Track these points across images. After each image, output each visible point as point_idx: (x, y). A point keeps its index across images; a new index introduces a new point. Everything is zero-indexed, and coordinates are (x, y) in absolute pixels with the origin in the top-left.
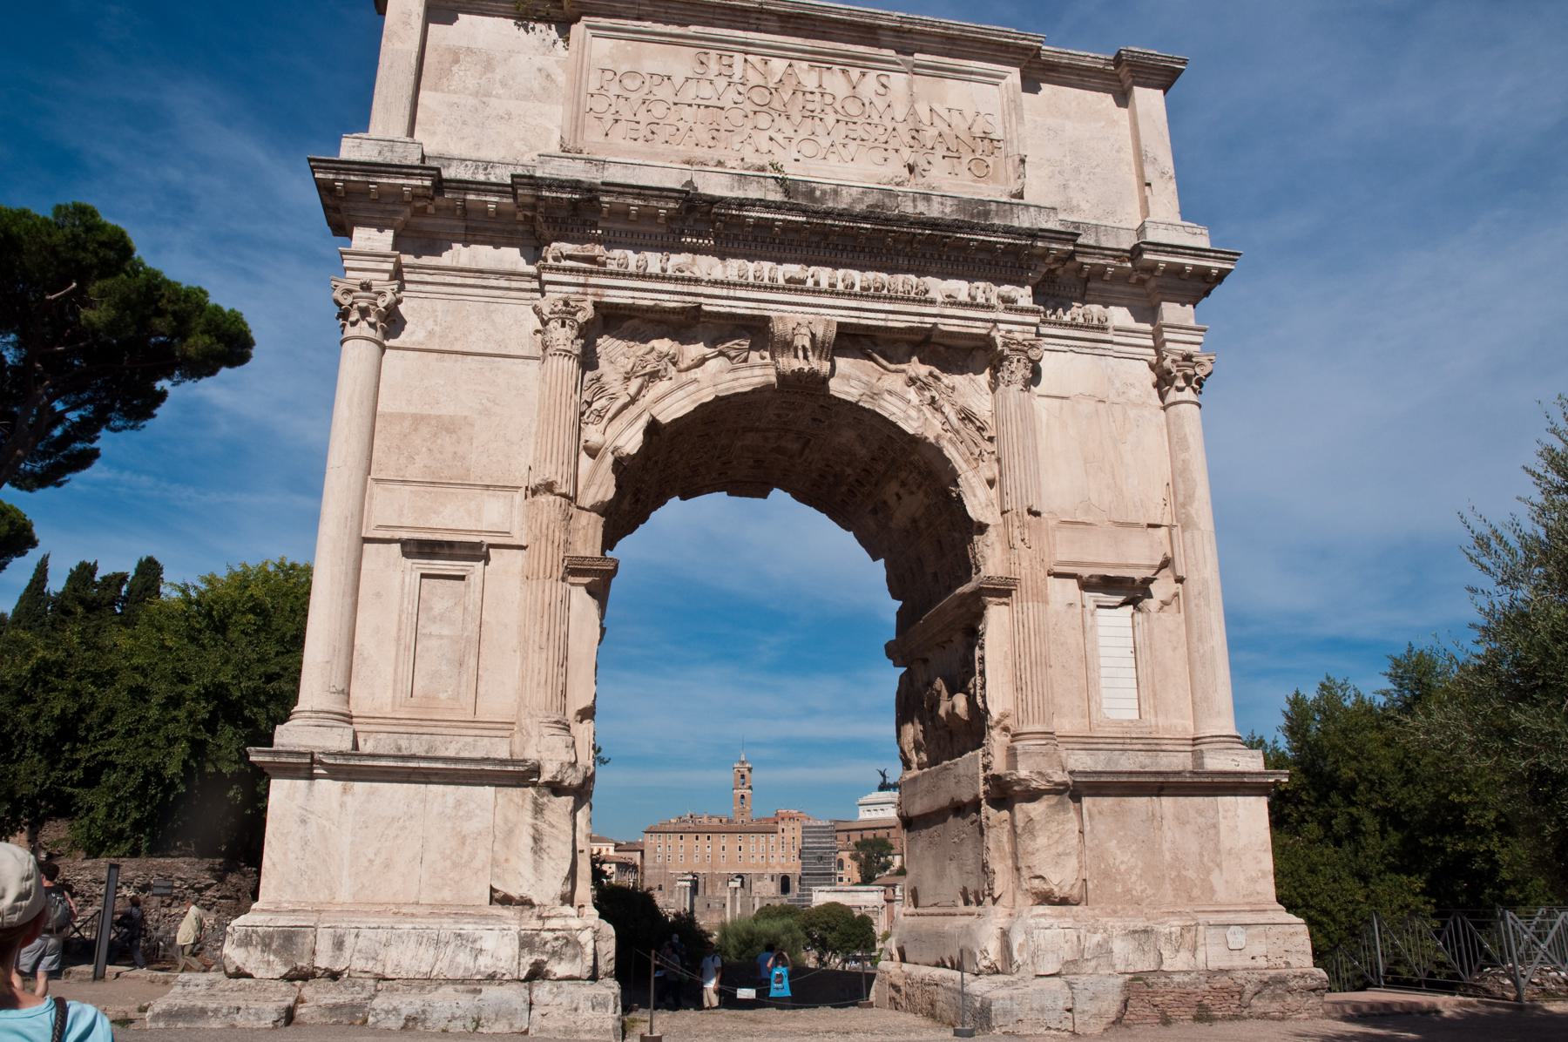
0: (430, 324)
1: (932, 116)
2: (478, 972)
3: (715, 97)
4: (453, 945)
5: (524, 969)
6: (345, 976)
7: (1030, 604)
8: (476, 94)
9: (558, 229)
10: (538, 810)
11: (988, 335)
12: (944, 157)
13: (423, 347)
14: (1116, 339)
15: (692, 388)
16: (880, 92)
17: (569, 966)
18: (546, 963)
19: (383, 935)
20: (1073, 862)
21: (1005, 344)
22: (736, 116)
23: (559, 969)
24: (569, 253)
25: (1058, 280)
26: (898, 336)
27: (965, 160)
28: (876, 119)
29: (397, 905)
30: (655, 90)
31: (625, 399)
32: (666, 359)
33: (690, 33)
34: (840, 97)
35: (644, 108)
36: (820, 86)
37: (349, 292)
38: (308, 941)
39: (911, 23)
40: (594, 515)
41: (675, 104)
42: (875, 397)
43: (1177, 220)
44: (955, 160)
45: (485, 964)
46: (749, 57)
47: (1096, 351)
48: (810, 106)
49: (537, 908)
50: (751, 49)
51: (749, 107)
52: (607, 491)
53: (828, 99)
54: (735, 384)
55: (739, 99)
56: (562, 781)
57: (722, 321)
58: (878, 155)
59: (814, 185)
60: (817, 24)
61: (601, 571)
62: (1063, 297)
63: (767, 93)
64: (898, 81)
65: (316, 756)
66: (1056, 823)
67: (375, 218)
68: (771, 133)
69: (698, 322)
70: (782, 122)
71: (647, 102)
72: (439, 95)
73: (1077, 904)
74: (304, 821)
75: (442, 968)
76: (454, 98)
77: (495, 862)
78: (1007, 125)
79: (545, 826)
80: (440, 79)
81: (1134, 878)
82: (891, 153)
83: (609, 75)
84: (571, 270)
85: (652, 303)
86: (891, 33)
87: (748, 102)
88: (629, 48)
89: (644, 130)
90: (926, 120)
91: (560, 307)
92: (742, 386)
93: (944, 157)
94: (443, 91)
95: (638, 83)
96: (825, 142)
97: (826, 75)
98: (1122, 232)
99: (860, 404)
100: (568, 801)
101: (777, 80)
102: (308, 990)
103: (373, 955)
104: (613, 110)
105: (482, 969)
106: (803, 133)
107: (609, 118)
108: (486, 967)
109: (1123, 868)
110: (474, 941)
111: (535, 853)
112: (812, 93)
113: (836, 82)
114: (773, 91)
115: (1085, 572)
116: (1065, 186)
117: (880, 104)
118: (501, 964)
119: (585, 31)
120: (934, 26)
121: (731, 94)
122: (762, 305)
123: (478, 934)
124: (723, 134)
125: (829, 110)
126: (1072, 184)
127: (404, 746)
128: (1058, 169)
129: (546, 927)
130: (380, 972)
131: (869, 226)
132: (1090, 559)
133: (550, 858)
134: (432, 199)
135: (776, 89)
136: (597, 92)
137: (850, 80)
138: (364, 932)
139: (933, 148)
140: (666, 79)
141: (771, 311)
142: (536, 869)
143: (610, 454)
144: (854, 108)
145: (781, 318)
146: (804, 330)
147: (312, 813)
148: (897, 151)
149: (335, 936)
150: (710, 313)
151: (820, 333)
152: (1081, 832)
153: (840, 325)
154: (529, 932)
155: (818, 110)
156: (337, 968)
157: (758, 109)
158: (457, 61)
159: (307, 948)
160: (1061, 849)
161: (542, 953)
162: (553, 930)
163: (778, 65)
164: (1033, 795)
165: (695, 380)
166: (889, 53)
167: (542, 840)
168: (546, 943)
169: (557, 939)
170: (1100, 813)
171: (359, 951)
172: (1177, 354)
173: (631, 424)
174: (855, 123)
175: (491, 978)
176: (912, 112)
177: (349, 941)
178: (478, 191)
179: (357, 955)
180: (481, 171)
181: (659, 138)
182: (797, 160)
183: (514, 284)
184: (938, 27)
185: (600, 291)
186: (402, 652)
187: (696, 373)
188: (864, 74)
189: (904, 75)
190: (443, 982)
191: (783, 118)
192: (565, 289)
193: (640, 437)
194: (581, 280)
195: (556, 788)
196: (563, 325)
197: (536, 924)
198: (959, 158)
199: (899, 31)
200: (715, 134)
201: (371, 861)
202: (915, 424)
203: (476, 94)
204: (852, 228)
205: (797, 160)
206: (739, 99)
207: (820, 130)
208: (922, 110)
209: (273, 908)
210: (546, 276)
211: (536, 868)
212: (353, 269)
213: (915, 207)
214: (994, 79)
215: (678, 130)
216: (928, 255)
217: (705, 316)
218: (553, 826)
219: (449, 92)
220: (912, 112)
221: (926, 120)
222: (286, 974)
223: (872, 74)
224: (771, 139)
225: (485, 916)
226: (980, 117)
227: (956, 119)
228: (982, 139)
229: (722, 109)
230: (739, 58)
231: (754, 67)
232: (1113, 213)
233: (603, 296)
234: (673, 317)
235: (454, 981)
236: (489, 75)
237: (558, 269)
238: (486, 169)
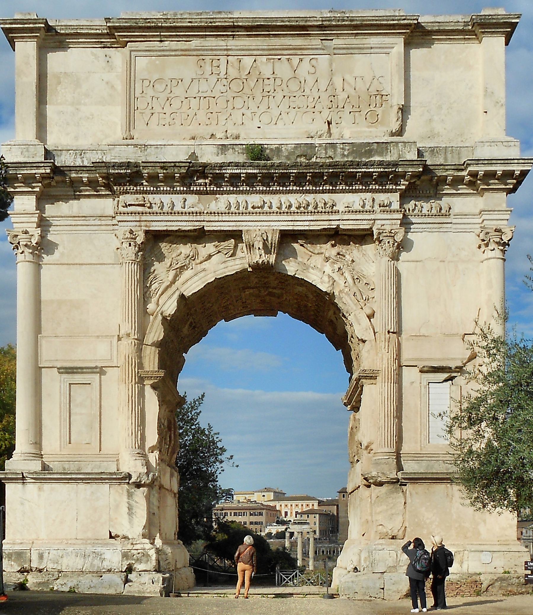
2: (104, 568)
3: (209, 91)
4: (91, 557)
5: (124, 567)
6: (45, 570)
7: (386, 384)
10: (130, 495)
11: (371, 228)
12: (350, 113)
14: (454, 221)
15: (202, 274)
17: (145, 565)
18: (134, 564)
19: (60, 553)
20: (400, 518)
21: (379, 234)
22: (221, 102)
23: (140, 567)
24: (130, 203)
25: (418, 187)
26: (319, 233)
27: (364, 113)
28: (307, 92)
29: (67, 540)
33: (192, 48)
36: (274, 73)
38: (27, 556)
39: (329, 21)
40: (153, 348)
41: (187, 98)
42: (305, 271)
43: (502, 136)
44: (357, 114)
45: (106, 565)
47: (441, 230)
49: (131, 540)
50: (230, 53)
51: (230, 94)
52: (159, 335)
53: (278, 82)
54: (226, 270)
56: (140, 481)
57: (218, 234)
58: (308, 118)
59: (266, 146)
61: (158, 377)
64: (323, 60)
65: (24, 475)
66: (391, 499)
68: (244, 110)
69: (206, 235)
70: (251, 103)
71: (170, 99)
73: (403, 539)
74: (22, 504)
75: (87, 567)
77: (111, 520)
78: (393, 84)
79: (133, 502)
81: (434, 526)
88: (157, 62)
89: (168, 119)
91: (127, 236)
92: (229, 271)
95: (164, 86)
96: (275, 112)
97: (277, 64)
99: (296, 276)
100: (144, 491)
102: (29, 577)
103: (57, 562)
105: (105, 567)
106: (263, 108)
107: (148, 112)
108: (107, 566)
109: (428, 521)
110: (101, 555)
111: (129, 515)
112: (268, 79)
114: (245, 81)
115: (421, 365)
117: (311, 80)
118: (114, 565)
120: (344, 20)
121: (220, 87)
123: (102, 552)
125: (278, 89)
127: (66, 468)
129: (134, 548)
130: (60, 569)
131: (296, 171)
132: (425, 356)
133: (136, 517)
134: (53, 178)
136: (140, 95)
137: (292, 67)
138: (51, 552)
139: (344, 107)
140: (180, 81)
142: (130, 522)
143: (160, 315)
145: (247, 231)
146: (259, 238)
147: (25, 500)
149: (39, 554)
150: (209, 231)
152: (405, 503)
153: (280, 230)
154: (126, 551)
156: (41, 567)
159: (28, 559)
160: (393, 511)
161: (132, 560)
162: (137, 550)
163: (248, 61)
164: (380, 484)
165: (204, 270)
166: (316, 42)
167: (132, 509)
168: (134, 555)
169: (139, 553)
170: (417, 493)
171: (50, 560)
173: (170, 298)
174: (295, 97)
175: (109, 571)
176: (331, 83)
177: (46, 555)
178: (77, 172)
179: (49, 561)
181: (178, 122)
182: (259, 127)
183: (103, 223)
185: (148, 224)
186: (62, 423)
187: (205, 265)
188: (301, 60)
190: (88, 573)
193: (175, 304)
195: (138, 485)
196: (130, 244)
197: (130, 547)
199: (322, 27)
201: (54, 521)
202: (327, 285)
204: (286, 173)
205: (259, 127)
206: (224, 89)
207: (273, 105)
208: (338, 82)
209: (11, 542)
210: (119, 218)
211: (131, 521)
213: (326, 153)
214: (386, 50)
216: (334, 183)
217: (208, 232)
218: (137, 503)
220: (331, 83)
222: (19, 570)
223: (307, 59)
225: (107, 544)
227: (360, 84)
228: (376, 96)
229: (214, 97)
230: (223, 59)
232: (461, 135)
233: (150, 226)
235: (93, 572)
238: (81, 155)
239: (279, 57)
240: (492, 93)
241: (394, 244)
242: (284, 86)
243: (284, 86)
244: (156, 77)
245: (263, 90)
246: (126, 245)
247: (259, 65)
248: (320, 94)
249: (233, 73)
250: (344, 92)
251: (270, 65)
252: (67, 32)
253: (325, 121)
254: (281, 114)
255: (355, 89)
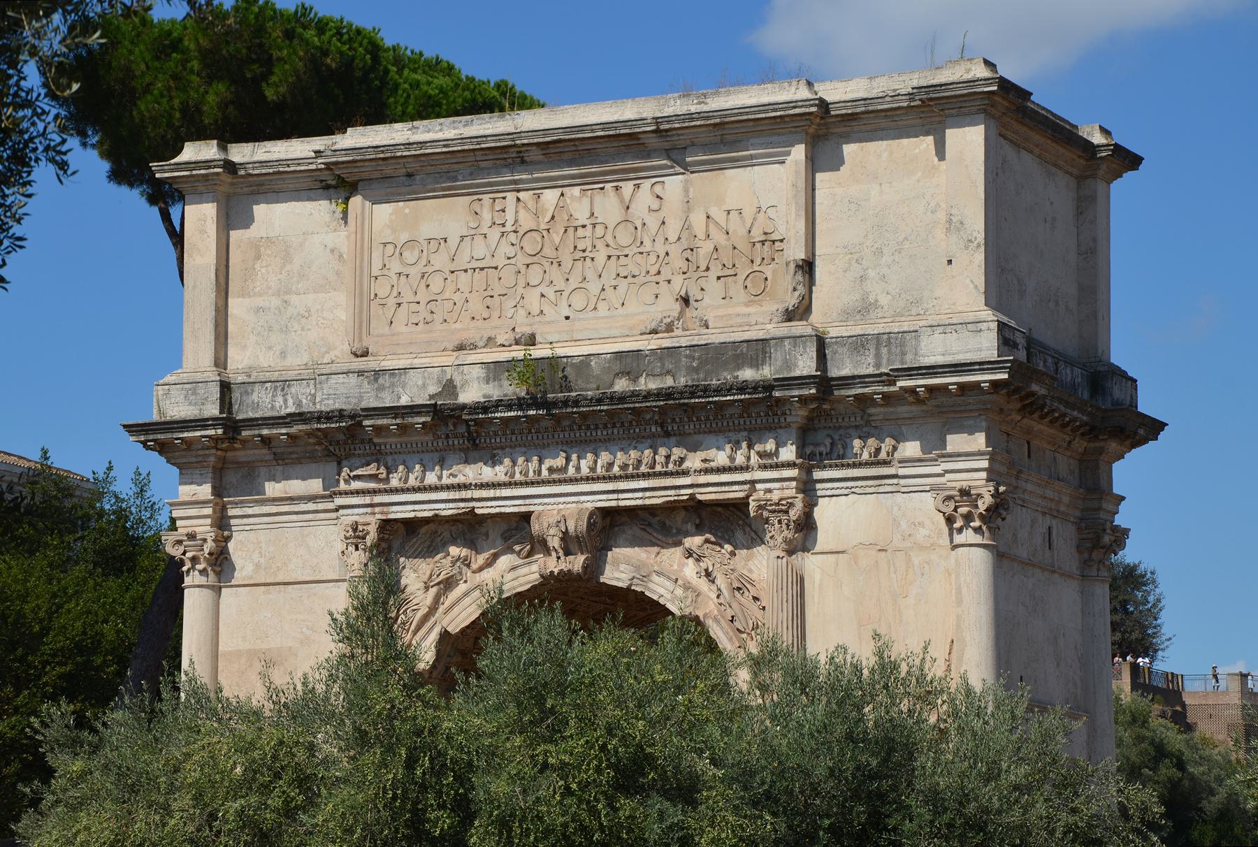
0: (256, 557)
1: (707, 226)
3: (489, 256)
8: (278, 294)
9: (342, 450)
13: (252, 582)
16: (652, 208)
22: (508, 275)
28: (648, 246)
30: (432, 257)
31: (424, 610)
32: (458, 564)
34: (611, 227)
35: (423, 282)
37: (179, 542)
39: (668, 122)
41: (452, 272)
44: (731, 278)
46: (522, 195)
48: (581, 246)
51: (521, 260)
53: (599, 231)
55: (511, 251)
60: (577, 143)
62: (847, 428)
63: (539, 239)
64: (674, 185)
67: (192, 463)
70: (555, 274)
71: (426, 275)
72: (247, 301)
76: (260, 302)
80: (246, 280)
82: (664, 285)
83: (390, 248)
84: (357, 492)
85: (430, 514)
86: (654, 135)
87: (519, 253)
88: (407, 211)
89: (424, 314)
90: (701, 234)
93: (719, 278)
94: (250, 297)
95: (416, 253)
96: (594, 287)
97: (598, 198)
98: (908, 336)
101: (548, 218)
104: (395, 293)
106: (574, 283)
107: (392, 302)
113: (607, 204)
114: (545, 233)
116: (863, 278)
117: (653, 224)
119: (363, 202)
120: (692, 119)
121: (506, 250)
122: (528, 501)
124: (497, 298)
125: (600, 244)
126: (871, 273)
128: (855, 256)
135: (548, 230)
136: (379, 273)
140: (442, 242)
141: (535, 507)
144: (624, 238)
148: (669, 282)
151: (571, 529)
155: (589, 249)
157: (529, 260)
158: (258, 257)
163: (550, 196)
172: (954, 488)
174: (626, 256)
176: (687, 226)
180: (279, 393)
181: (438, 318)
184: (698, 119)
185: (385, 509)
189: (680, 176)
191: (555, 265)
192: (356, 511)
194: (367, 500)
196: (357, 549)
198: (735, 275)
200: (489, 301)
203: (278, 293)
205: (567, 318)
206: (511, 251)
207: (590, 275)
208: (698, 220)
212: (182, 518)
215: (455, 304)
219: (254, 295)
220: (687, 226)
221: (701, 234)
223: (647, 184)
224: (543, 296)
226: (762, 213)
227: (735, 224)
229: (496, 268)
230: (511, 197)
231: (526, 207)
232: (917, 302)
234: (462, 517)
236: (288, 267)
237: (346, 493)
238: (283, 389)
239: (601, 185)
240: (962, 223)
241: (788, 525)
242: (609, 238)
243: (609, 238)
244: (404, 237)
245: (575, 247)
246: (352, 548)
247: (568, 201)
248: (667, 248)
249: (526, 222)
250: (708, 241)
251: (586, 201)
252: (264, 171)
253: (676, 297)
254: (603, 290)
255: (728, 233)
